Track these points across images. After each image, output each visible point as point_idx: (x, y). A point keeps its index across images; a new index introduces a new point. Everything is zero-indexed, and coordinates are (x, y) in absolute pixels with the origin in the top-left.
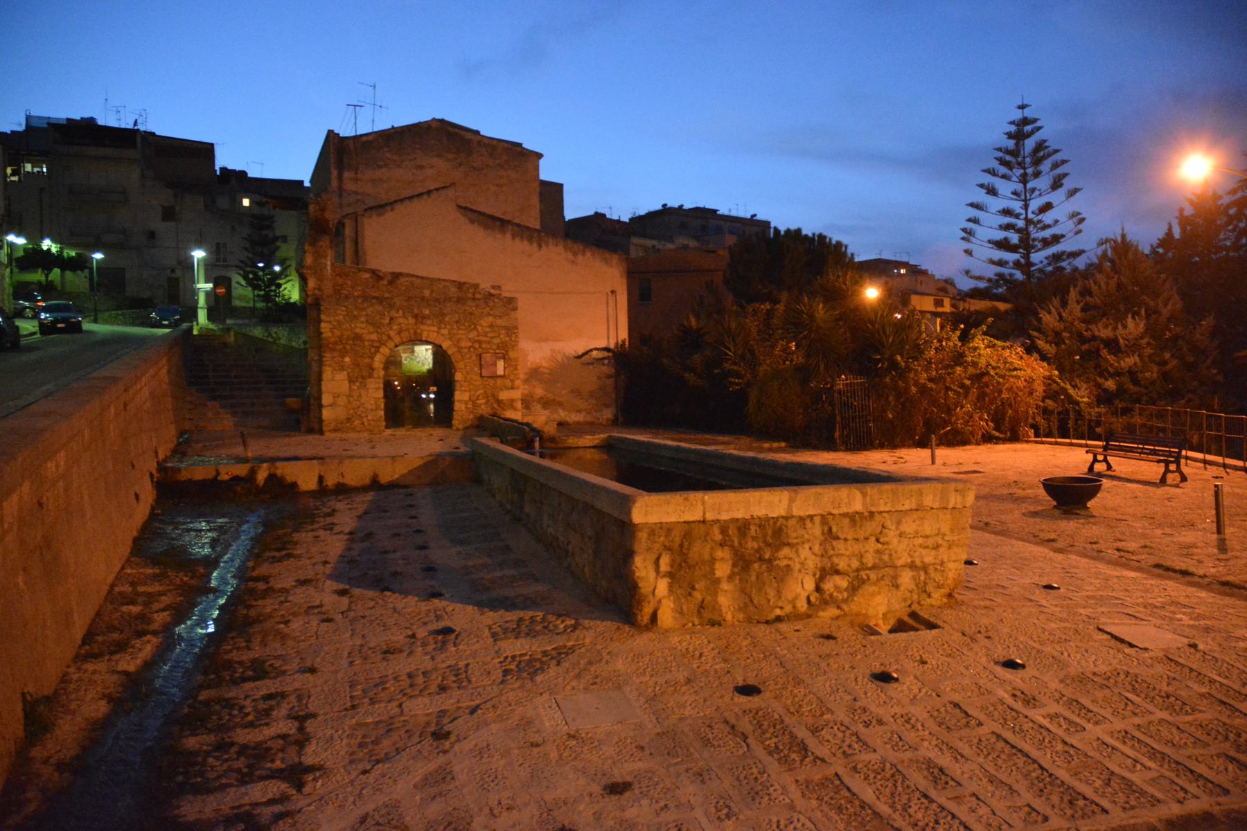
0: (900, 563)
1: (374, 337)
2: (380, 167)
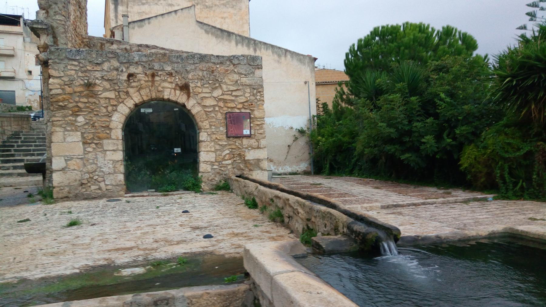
1: (112, 95)
2: (143, 4)
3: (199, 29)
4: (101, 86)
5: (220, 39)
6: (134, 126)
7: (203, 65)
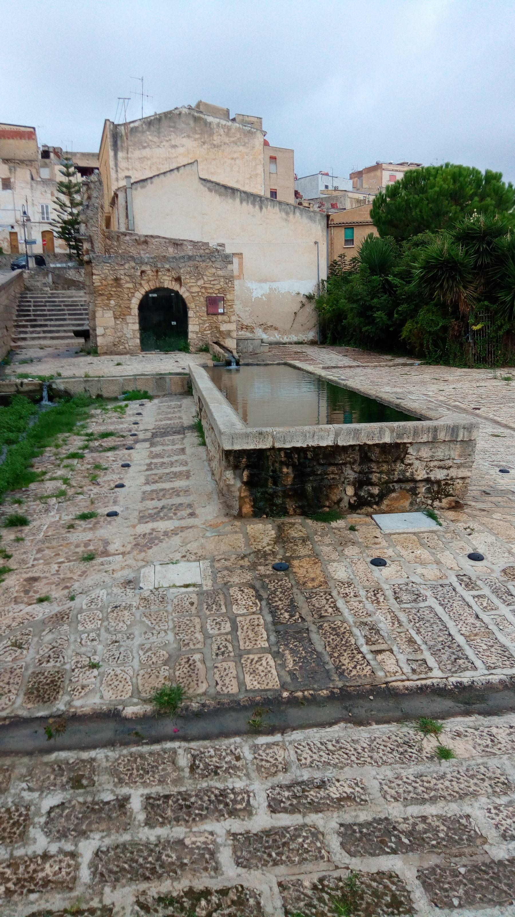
0: (419, 478)
1: (130, 285)
2: (144, 148)
3: (202, 187)
4: (124, 279)
5: (223, 197)
6: (145, 305)
7: (191, 263)
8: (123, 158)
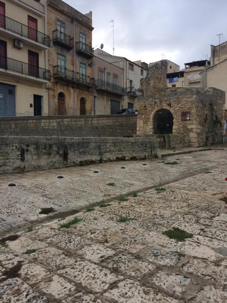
1: (150, 109)
7: (175, 97)
8: (217, 60)
